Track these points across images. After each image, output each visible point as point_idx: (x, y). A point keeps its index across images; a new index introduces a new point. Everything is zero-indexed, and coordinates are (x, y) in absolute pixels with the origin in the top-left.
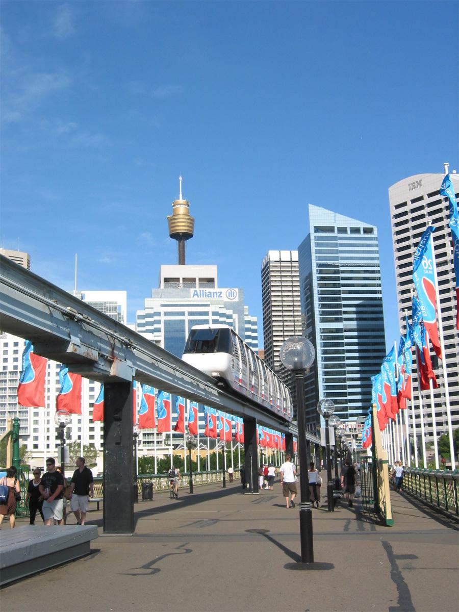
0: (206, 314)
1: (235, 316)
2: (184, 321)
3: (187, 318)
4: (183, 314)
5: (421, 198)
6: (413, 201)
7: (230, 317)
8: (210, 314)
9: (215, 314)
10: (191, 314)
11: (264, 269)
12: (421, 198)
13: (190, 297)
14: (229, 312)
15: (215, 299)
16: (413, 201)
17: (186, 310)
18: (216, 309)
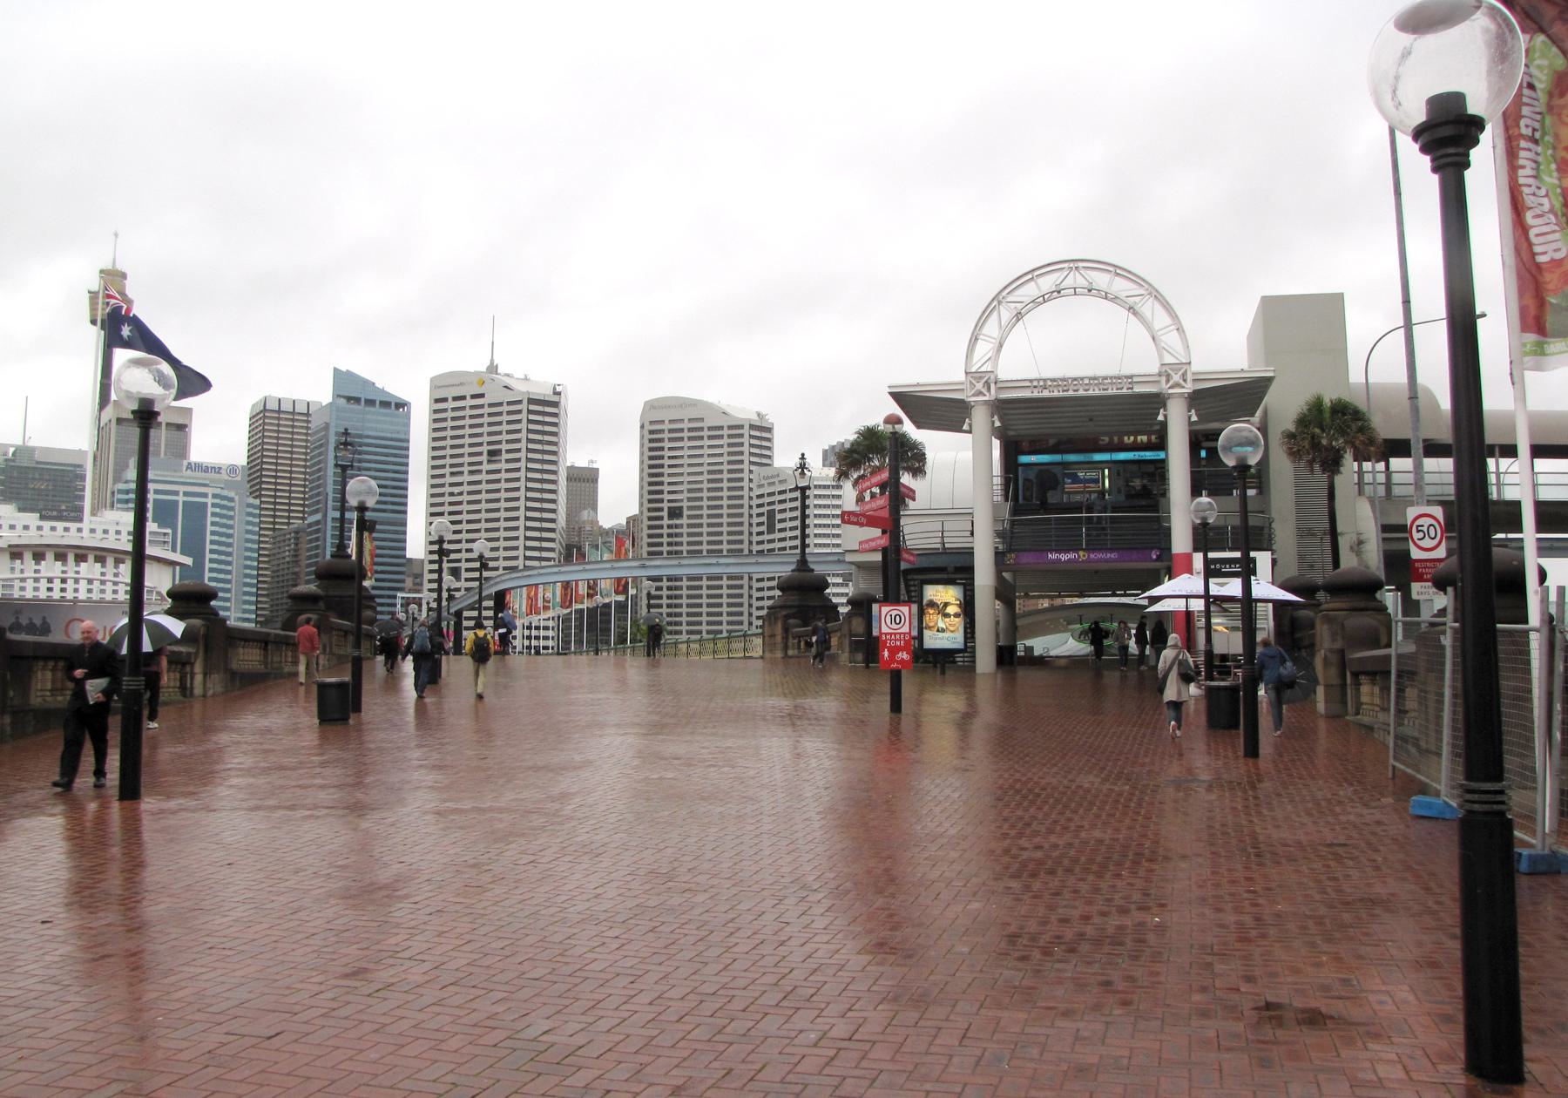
0: (205, 495)
1: (237, 498)
2: (177, 502)
3: (181, 499)
4: (176, 493)
5: (463, 398)
6: (455, 399)
7: (232, 500)
8: (210, 496)
9: (215, 496)
10: (186, 494)
11: (254, 417)
12: (463, 398)
13: (181, 471)
14: (232, 494)
15: (213, 475)
16: (455, 399)
17: (182, 489)
18: (218, 491)
